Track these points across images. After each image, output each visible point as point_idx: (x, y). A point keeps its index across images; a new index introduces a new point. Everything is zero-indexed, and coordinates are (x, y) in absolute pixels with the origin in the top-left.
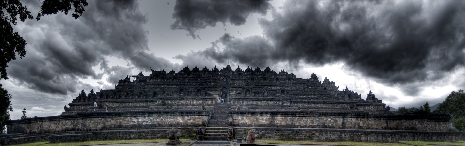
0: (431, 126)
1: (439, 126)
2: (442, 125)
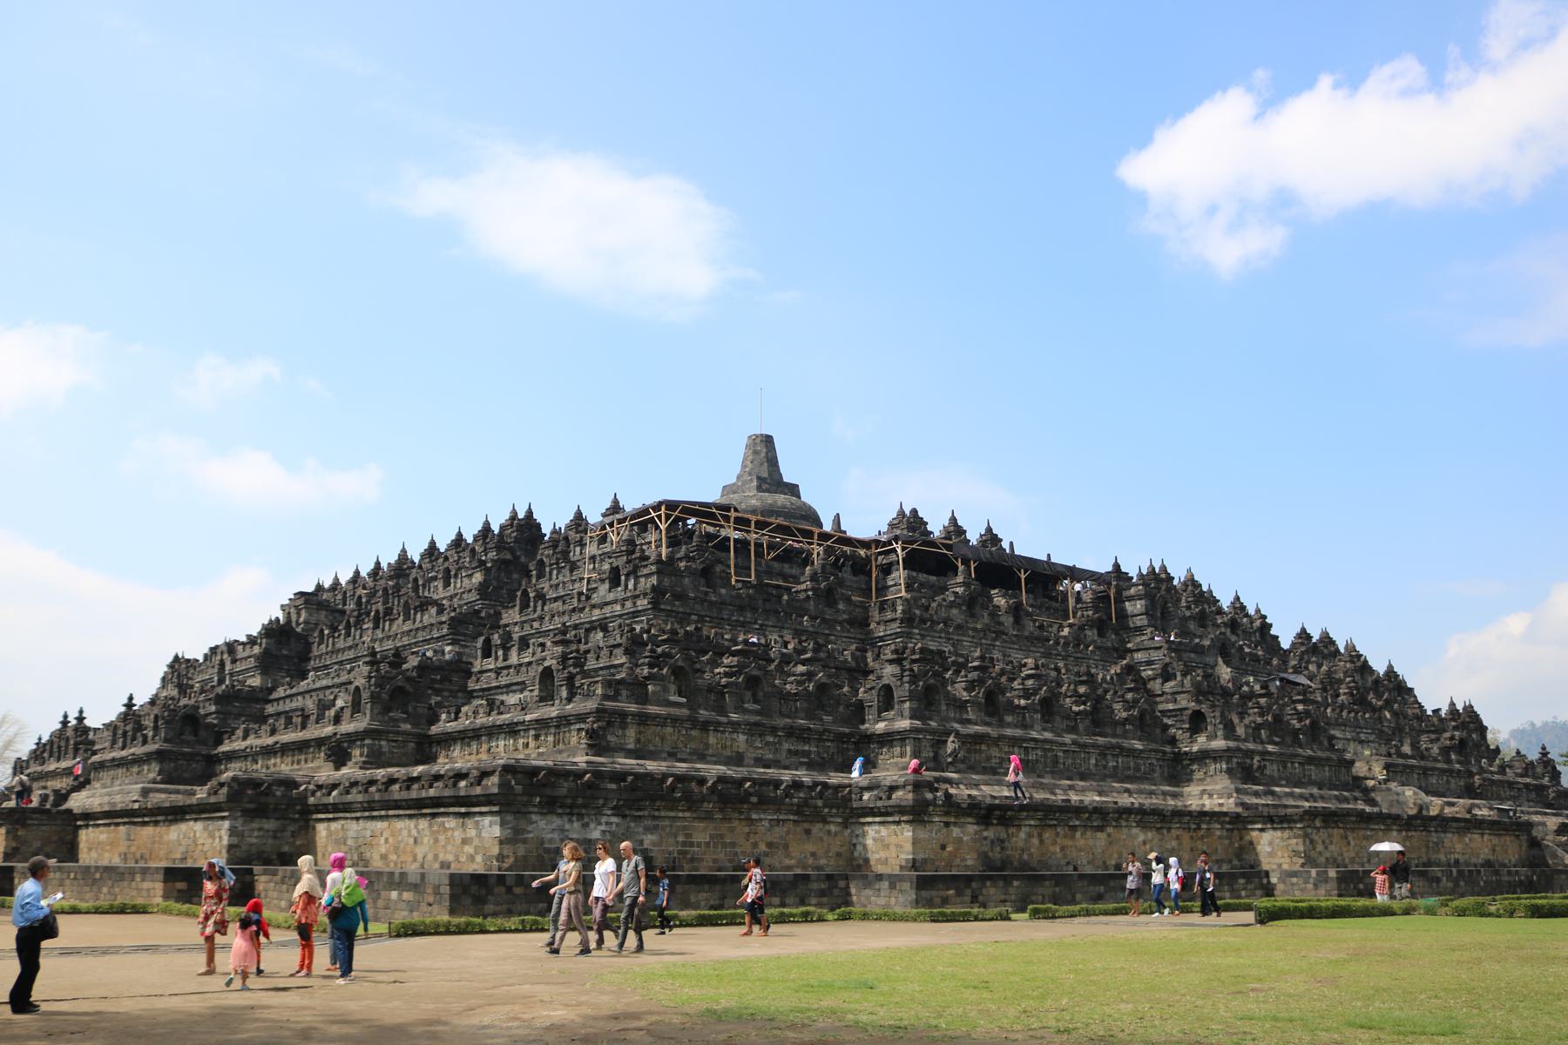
0: (391, 840)
1: (436, 841)
2: (450, 833)
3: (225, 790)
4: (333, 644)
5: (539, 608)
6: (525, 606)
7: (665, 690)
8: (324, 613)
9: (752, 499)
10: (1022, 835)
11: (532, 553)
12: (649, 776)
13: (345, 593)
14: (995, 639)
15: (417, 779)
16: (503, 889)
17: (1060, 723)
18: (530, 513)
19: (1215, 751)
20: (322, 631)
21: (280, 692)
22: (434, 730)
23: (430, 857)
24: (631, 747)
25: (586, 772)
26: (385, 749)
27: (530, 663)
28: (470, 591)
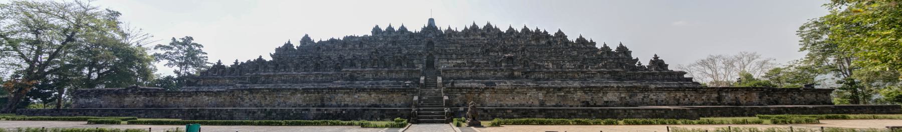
10: (160, 99)
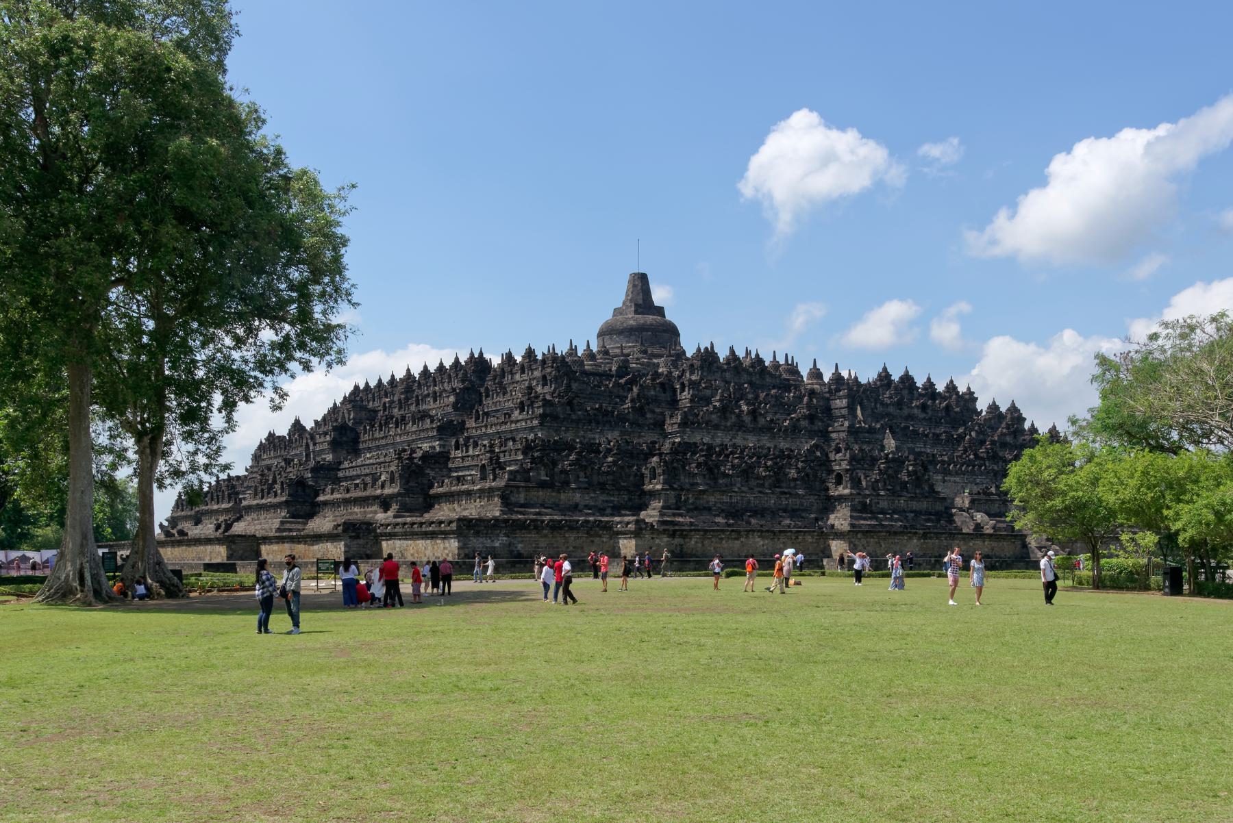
1: (433, 548)
3: (341, 528)
4: (373, 435)
5: (485, 420)
6: (477, 418)
7: (539, 474)
8: (364, 412)
9: (632, 319)
10: (693, 542)
11: (483, 380)
12: (519, 520)
13: (374, 393)
14: (738, 431)
15: (424, 523)
16: (458, 566)
17: (753, 483)
18: (481, 354)
19: (845, 495)
20: (365, 427)
21: (346, 465)
22: (432, 492)
23: (431, 554)
24: (522, 502)
25: (492, 520)
26: (408, 502)
27: (479, 455)
28: (448, 406)
